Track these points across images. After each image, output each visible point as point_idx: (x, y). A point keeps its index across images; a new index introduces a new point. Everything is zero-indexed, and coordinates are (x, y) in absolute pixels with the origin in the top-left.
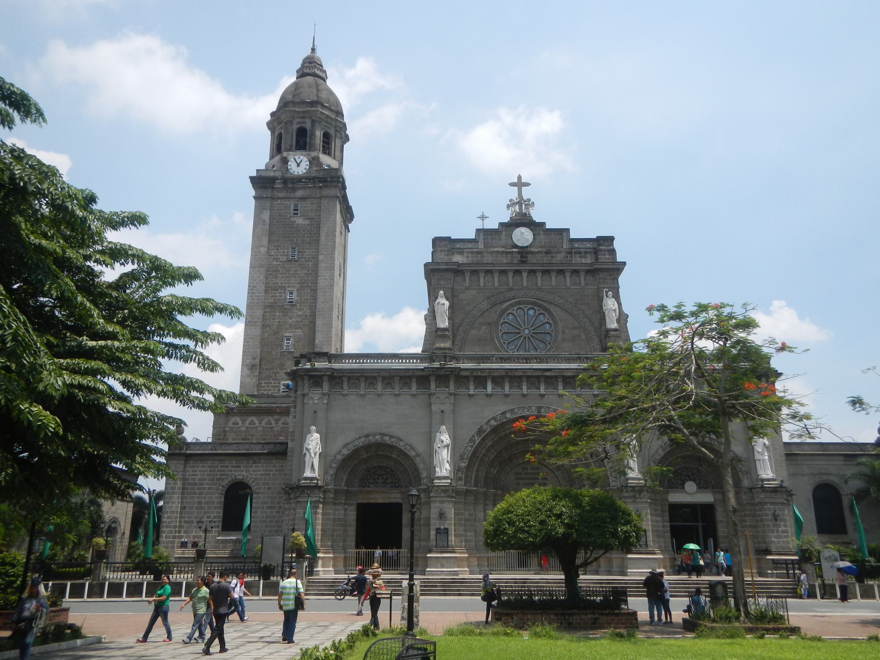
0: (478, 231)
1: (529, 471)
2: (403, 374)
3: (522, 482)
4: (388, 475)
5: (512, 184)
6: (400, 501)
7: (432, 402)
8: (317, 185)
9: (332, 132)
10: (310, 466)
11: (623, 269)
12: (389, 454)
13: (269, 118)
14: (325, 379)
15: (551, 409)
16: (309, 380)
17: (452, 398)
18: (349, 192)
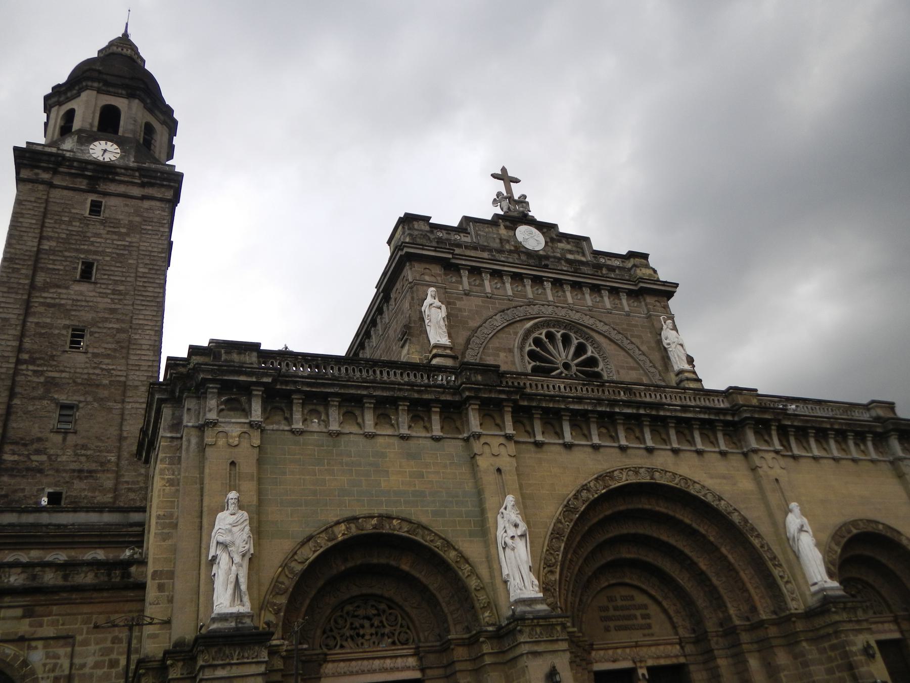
0: (466, 220)
1: (620, 603)
2: (416, 396)
3: (612, 624)
4: (384, 619)
5: (495, 176)
6: (417, 675)
7: (476, 451)
8: (139, 181)
9: (157, 125)
10: (231, 587)
11: (673, 295)
12: (393, 563)
13: (49, 91)
14: (258, 392)
15: (668, 473)
16: (220, 394)
17: (512, 448)
18: (178, 209)
